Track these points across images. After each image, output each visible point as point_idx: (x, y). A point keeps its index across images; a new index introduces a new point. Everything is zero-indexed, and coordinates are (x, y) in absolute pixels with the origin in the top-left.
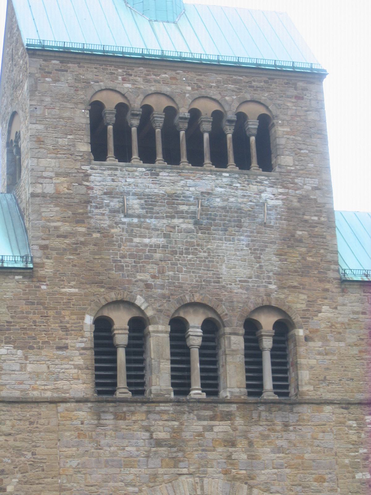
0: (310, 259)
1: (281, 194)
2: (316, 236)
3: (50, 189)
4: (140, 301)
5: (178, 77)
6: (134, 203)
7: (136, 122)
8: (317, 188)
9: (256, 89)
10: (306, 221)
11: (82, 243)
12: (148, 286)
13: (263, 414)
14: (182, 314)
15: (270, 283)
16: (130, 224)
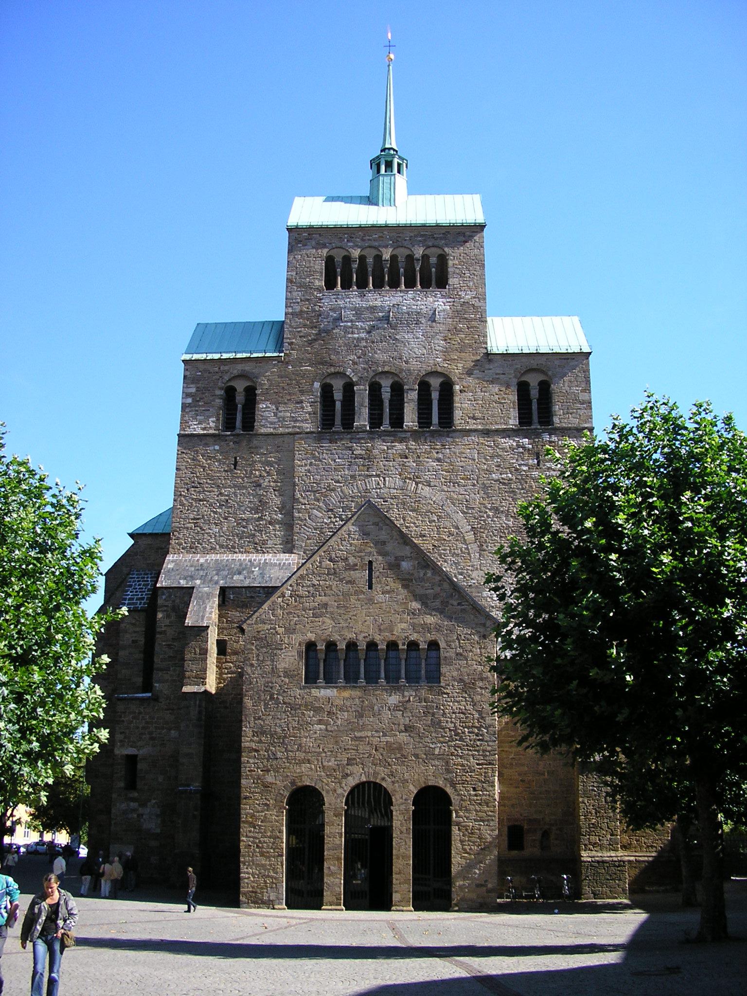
0: (467, 341)
1: (447, 302)
2: (472, 327)
3: (297, 309)
4: (349, 372)
5: (384, 236)
6: (348, 314)
7: (355, 266)
8: (474, 298)
9: (436, 239)
10: (465, 318)
11: (315, 340)
12: (355, 363)
13: (428, 438)
14: (377, 380)
15: (438, 358)
16: (345, 326)
